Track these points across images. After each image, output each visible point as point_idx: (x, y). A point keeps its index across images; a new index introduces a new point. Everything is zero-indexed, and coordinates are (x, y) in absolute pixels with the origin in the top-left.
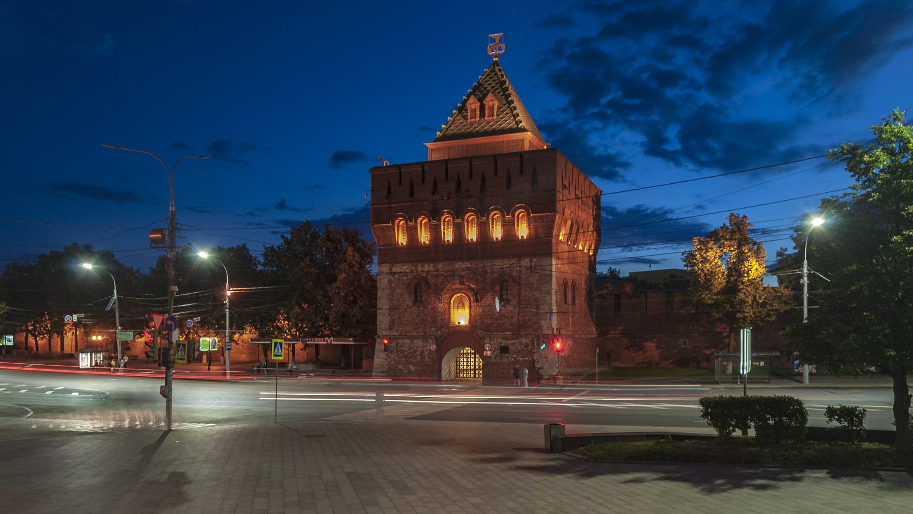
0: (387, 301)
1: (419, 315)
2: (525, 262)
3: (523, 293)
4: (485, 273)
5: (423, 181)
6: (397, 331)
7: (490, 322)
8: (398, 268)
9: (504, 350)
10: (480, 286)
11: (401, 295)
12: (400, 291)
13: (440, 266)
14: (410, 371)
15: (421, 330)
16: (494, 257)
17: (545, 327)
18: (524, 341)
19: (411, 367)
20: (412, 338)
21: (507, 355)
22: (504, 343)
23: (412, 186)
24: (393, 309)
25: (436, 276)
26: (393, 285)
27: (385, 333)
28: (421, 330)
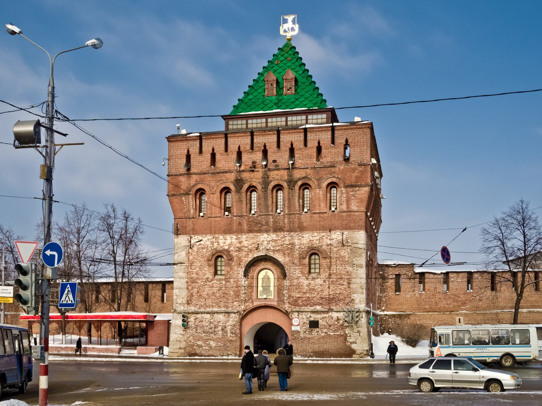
0: (184, 275)
1: (219, 290)
2: (337, 235)
3: (333, 267)
4: (293, 244)
6: (195, 306)
7: (298, 295)
9: (314, 324)
10: (287, 259)
13: (244, 237)
14: (211, 347)
15: (222, 304)
16: (302, 229)
17: (357, 301)
18: (335, 315)
19: (213, 344)
20: (212, 313)
21: (317, 329)
22: (314, 317)
23: (213, 155)
25: (239, 249)
26: (191, 257)
28: (222, 304)
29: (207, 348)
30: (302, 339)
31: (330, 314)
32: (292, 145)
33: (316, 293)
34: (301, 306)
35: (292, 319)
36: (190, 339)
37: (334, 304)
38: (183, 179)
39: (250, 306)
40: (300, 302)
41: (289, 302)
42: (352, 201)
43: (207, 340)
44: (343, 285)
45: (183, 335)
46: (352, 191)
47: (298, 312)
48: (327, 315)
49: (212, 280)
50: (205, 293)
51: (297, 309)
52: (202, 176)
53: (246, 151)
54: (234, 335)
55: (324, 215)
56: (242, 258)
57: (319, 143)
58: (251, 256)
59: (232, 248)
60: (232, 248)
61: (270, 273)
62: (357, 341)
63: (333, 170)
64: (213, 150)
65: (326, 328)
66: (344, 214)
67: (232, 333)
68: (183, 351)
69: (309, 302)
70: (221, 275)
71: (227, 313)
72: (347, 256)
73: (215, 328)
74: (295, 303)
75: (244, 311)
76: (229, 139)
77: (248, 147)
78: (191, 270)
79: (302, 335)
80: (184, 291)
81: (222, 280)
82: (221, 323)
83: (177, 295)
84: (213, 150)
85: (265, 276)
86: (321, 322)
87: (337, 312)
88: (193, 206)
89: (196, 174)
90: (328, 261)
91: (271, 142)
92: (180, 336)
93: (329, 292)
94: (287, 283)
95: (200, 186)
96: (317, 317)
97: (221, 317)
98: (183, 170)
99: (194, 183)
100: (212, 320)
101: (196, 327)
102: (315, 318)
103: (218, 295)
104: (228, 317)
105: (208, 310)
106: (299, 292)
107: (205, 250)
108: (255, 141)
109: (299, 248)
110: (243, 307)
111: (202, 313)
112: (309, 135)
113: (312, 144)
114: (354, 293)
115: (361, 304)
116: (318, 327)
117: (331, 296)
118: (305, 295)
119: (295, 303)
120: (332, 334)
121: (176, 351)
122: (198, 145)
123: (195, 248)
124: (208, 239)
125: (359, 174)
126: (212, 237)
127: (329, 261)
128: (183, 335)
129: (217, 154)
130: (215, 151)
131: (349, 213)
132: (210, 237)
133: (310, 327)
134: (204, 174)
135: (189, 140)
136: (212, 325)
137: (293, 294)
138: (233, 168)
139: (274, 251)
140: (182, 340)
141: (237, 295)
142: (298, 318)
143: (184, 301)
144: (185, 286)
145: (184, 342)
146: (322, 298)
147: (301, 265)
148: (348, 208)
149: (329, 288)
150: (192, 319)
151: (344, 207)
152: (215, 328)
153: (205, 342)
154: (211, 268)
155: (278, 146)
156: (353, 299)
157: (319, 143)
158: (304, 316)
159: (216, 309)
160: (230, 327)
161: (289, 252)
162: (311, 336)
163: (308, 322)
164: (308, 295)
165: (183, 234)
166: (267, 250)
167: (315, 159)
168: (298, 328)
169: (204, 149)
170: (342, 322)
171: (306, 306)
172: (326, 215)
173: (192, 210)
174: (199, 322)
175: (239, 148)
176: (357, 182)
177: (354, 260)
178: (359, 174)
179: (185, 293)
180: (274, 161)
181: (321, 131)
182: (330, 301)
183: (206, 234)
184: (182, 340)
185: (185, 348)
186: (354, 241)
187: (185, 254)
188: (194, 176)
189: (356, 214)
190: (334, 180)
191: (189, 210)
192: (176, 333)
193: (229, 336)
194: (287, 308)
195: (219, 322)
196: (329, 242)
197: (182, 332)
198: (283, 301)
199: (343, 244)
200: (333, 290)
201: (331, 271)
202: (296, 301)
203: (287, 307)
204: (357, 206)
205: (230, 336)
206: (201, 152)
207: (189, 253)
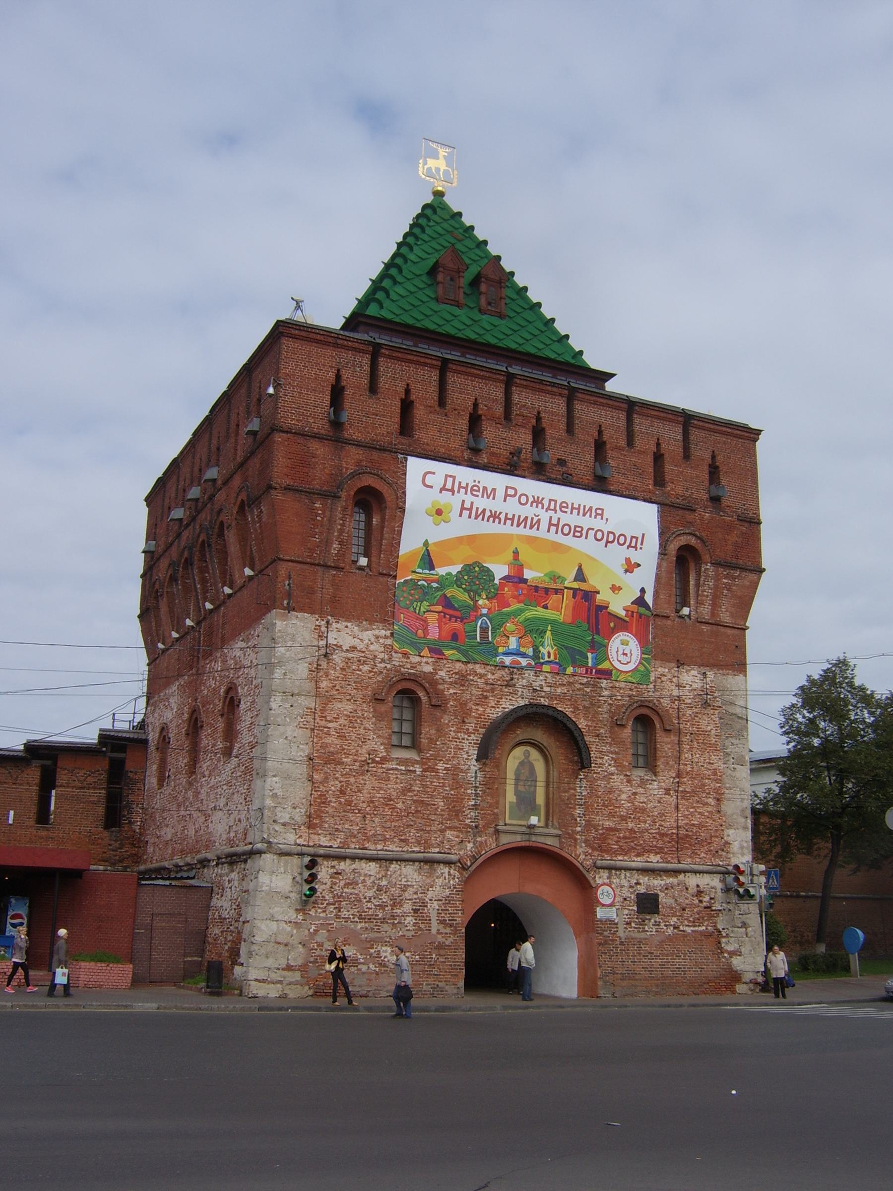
0: (302, 735)
1: (405, 791)
2: (691, 677)
5: (442, 402)
6: (333, 834)
7: (608, 824)
8: (346, 635)
9: (648, 904)
11: (352, 719)
12: (348, 707)
14: (382, 965)
18: (693, 881)
23: (407, 406)
24: (321, 760)
26: (324, 684)
27: (291, 837)
29: (371, 966)
30: (622, 943)
32: (600, 432)
34: (616, 853)
35: (598, 886)
36: (319, 938)
37: (689, 852)
38: (319, 449)
39: (491, 845)
40: (612, 840)
41: (586, 841)
42: (724, 601)
43: (372, 942)
44: (707, 804)
45: (297, 924)
46: (726, 577)
47: (610, 868)
49: (384, 760)
50: (364, 796)
52: (375, 455)
53: (492, 418)
54: (448, 930)
55: (664, 621)
56: (470, 705)
57: (658, 445)
58: (493, 704)
59: (442, 673)
60: (442, 673)
61: (535, 754)
62: (743, 950)
63: (689, 516)
64: (408, 391)
65: (674, 915)
66: (704, 628)
67: (442, 922)
68: (297, 976)
69: (633, 843)
70: (400, 746)
71: (426, 861)
72: (713, 732)
73: (393, 906)
74: (600, 845)
75: (474, 859)
76: (450, 375)
77: (499, 410)
78: (323, 723)
79: (621, 933)
80: (299, 784)
81: (417, 762)
82: (411, 890)
83: (275, 796)
84: (408, 391)
85: (522, 764)
86: (663, 899)
88: (341, 531)
89: (358, 445)
90: (674, 738)
91: (553, 413)
92: (288, 928)
94: (581, 788)
95: (368, 481)
97: (410, 874)
98: (320, 425)
99: (351, 469)
100: (384, 883)
101: (338, 901)
103: (400, 805)
104: (430, 874)
105: (373, 849)
106: (611, 815)
107: (366, 668)
108: (515, 398)
109: (611, 697)
110: (470, 846)
111: (353, 858)
112: (637, 419)
113: (645, 444)
114: (730, 827)
115: (743, 854)
116: (657, 912)
117: (682, 832)
118: (623, 825)
120: (689, 930)
121: (274, 976)
122: (367, 368)
123: (337, 658)
124: (377, 637)
125: (740, 540)
126: (388, 633)
127: (676, 739)
128: (297, 924)
129: (417, 405)
130: (413, 397)
131: (715, 627)
132: (383, 633)
134: (383, 450)
135: (343, 347)
136: (385, 898)
137: (598, 819)
138: (459, 453)
139: (551, 696)
140: (294, 941)
141: (455, 810)
143: (299, 815)
144: (302, 770)
145: (301, 949)
146: (662, 835)
147: (616, 741)
148: (713, 614)
149: (677, 808)
150: (324, 872)
151: (705, 611)
152: (393, 906)
153: (364, 950)
154: (383, 724)
155: (570, 429)
156: (727, 843)
157: (658, 445)
158: (624, 880)
159: (394, 848)
160: (435, 905)
161: (587, 704)
162: (643, 935)
163: (633, 896)
164: (631, 825)
165: (302, 610)
166: (535, 690)
167: (651, 482)
168: (612, 914)
169: (383, 382)
170: (707, 899)
171: (626, 854)
172: (669, 622)
173: (336, 546)
174: (347, 885)
175: (476, 405)
176: (737, 557)
177: (727, 743)
178: (740, 540)
179: (300, 792)
180: (562, 462)
181: (664, 419)
182: (680, 842)
183: (371, 621)
184: (294, 941)
185: (303, 968)
186: (726, 698)
187: (306, 672)
188: (353, 450)
189: (729, 631)
190: (693, 541)
191: (328, 543)
192: (272, 918)
193: (434, 931)
194: (582, 857)
195: (404, 889)
196: (676, 692)
197: (292, 915)
198: (571, 836)
199: (705, 701)
200: (685, 816)
201: (682, 767)
202: (603, 838)
203: (580, 855)
204: (732, 615)
205: (439, 932)
206: (373, 388)
207: (318, 669)
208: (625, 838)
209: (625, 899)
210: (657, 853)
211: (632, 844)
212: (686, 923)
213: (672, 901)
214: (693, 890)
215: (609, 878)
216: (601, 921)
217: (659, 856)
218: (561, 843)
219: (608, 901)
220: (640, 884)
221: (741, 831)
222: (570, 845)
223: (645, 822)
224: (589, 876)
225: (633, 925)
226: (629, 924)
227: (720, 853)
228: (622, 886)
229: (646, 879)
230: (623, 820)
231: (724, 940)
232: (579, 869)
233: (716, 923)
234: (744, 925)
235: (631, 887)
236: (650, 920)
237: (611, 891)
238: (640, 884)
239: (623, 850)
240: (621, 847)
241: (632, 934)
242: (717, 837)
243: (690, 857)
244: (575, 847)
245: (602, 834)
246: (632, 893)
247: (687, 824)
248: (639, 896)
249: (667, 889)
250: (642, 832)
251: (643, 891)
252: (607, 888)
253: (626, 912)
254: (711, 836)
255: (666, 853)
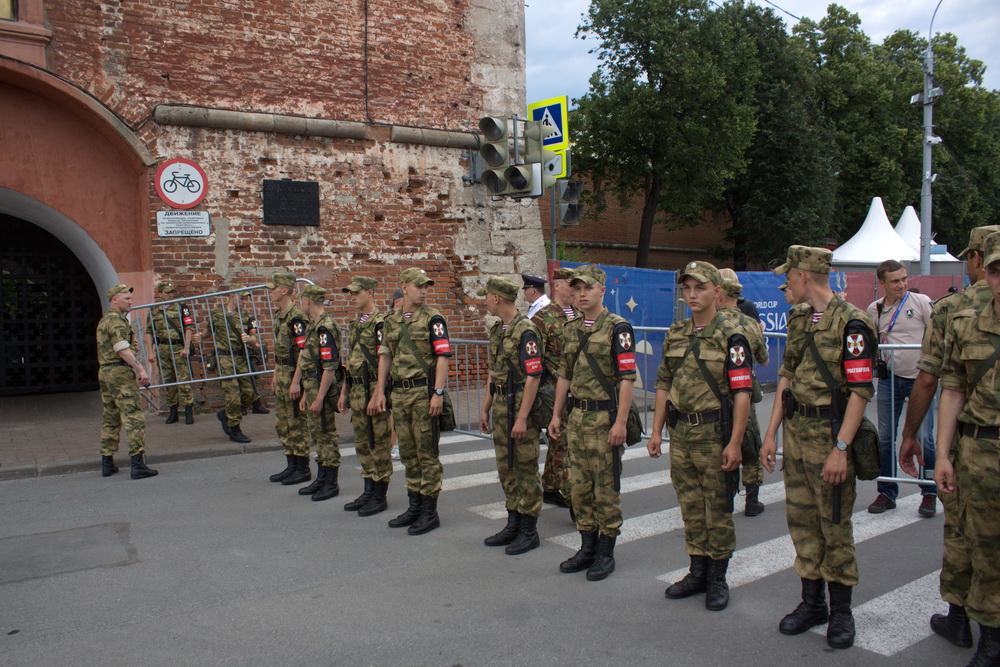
7: (187, 25)
9: (291, 205)
18: (400, 160)
21: (311, 235)
22: (286, 161)
31: (373, 151)
33: (296, 28)
34: (210, 92)
35: (160, 165)
40: (201, 66)
47: (195, 125)
48: (359, 158)
51: (189, 104)
65: (355, 229)
79: (222, 268)
87: (406, 142)
93: (365, 35)
96: (314, 162)
102: (293, 169)
114: (483, 59)
116: (315, 222)
117: (377, 59)
118: (232, 33)
119: (172, 66)
120: (390, 259)
133: (268, 220)
142: (194, 162)
146: (328, 61)
156: (476, 90)
158: (229, 151)
162: (280, 271)
163: (253, 188)
164: (249, 34)
168: (200, 224)
170: (433, 196)
171: (238, 96)
182: (374, 76)
194: (118, 96)
198: (86, 45)
200: (384, 28)
203: (112, 89)
208: (234, 59)
209: (235, 194)
210: (315, 99)
211: (254, 75)
212: (384, 244)
213: (352, 199)
214: (401, 177)
215: (191, 146)
216: (168, 241)
217: (320, 105)
218: (53, 59)
219: (190, 198)
220: (272, 162)
221: (505, 69)
222: (82, 68)
223: (287, 30)
224: (138, 142)
225: (254, 250)
226: (243, 247)
227: (462, 107)
228: (226, 166)
229: (290, 151)
230: (227, 20)
231: (467, 279)
232: (103, 121)
233: (451, 245)
234: (510, 250)
235: (249, 167)
236: (296, 239)
237: (195, 175)
238: (272, 162)
239: (231, 87)
240: (224, 79)
241: (250, 269)
242: (455, 76)
243: (395, 111)
244: (96, 72)
245: (170, 48)
246: (251, 181)
247: (386, 44)
248: (270, 187)
249: (339, 174)
250: (278, 51)
251: (280, 177)
252: (185, 169)
253: (237, 221)
254: (443, 74)
255: (338, 100)
